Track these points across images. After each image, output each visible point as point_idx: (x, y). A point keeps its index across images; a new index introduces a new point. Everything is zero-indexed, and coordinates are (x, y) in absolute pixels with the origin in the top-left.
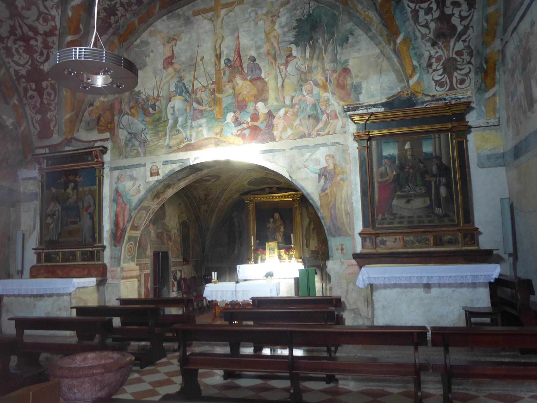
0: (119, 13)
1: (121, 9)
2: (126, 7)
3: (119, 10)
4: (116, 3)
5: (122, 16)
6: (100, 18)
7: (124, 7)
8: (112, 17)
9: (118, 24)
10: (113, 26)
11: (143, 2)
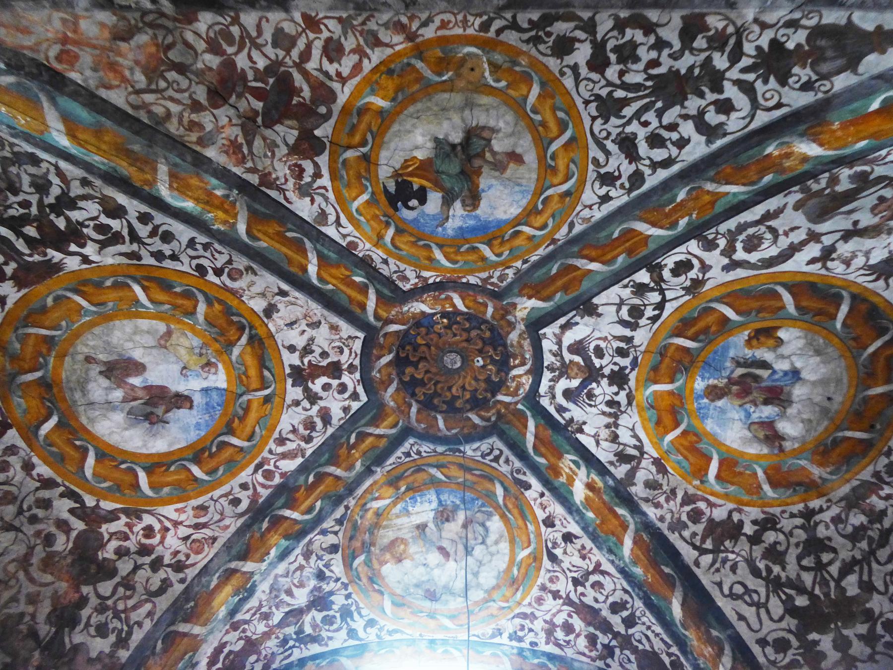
0: (764, 42)
1: (749, 48)
2: (732, 41)
3: (759, 48)
4: (744, 70)
5: (764, 26)
6: (817, 73)
7: (739, 45)
8: (791, 45)
9: (797, 15)
10: (812, 22)
11: (683, 18)
